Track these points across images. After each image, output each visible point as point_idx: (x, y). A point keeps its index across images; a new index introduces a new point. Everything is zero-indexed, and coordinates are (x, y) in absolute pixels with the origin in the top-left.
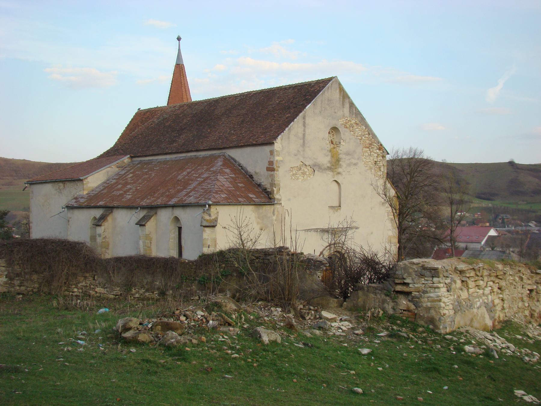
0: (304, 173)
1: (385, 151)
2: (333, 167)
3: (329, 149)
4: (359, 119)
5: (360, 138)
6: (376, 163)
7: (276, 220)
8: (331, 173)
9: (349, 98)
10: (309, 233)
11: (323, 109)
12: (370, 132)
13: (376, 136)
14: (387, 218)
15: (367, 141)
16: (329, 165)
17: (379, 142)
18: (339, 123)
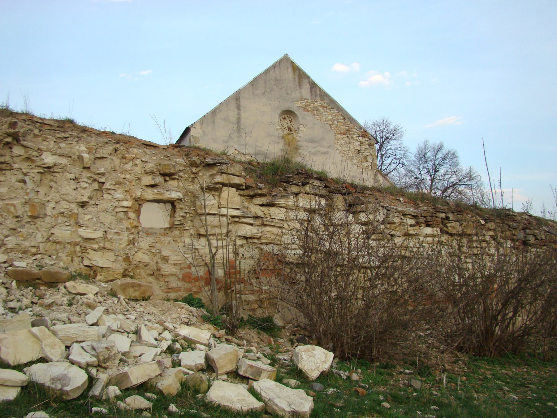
1: (371, 138)
3: (281, 135)
5: (331, 123)
6: (359, 152)
9: (308, 77)
11: (269, 90)
12: (346, 116)
15: (343, 127)
18: (295, 107)
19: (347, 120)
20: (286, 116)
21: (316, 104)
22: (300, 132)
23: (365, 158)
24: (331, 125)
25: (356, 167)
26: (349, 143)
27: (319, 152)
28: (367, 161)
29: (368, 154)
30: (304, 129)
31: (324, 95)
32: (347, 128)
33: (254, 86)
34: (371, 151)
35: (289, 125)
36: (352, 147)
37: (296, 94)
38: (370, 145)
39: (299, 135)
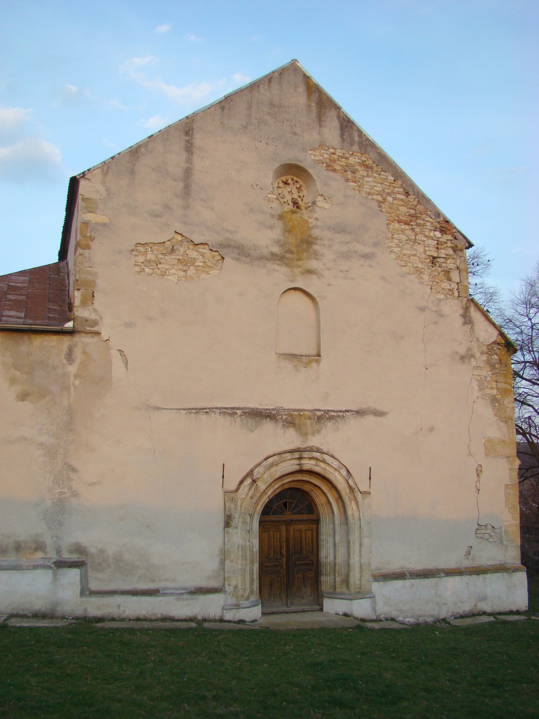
0: (186, 263)
2: (288, 255)
4: (373, 155)
5: (379, 198)
7: (76, 376)
8: (284, 270)
9: (338, 108)
10: (203, 417)
11: (255, 122)
12: (410, 189)
13: (428, 201)
14: (476, 393)
15: (403, 209)
16: (276, 249)
17: (438, 214)
18: (307, 160)
19: (411, 198)
20: (289, 177)
21: (352, 160)
22: (317, 209)
23: (447, 273)
24: (379, 202)
25: (428, 290)
26: (415, 241)
27: (355, 252)
28: (449, 279)
29: (452, 266)
30: (327, 206)
31: (367, 145)
32: (412, 212)
33: (226, 111)
34: (458, 261)
35: (295, 196)
36: (421, 249)
37: (311, 136)
38: (455, 249)
39: (316, 215)
